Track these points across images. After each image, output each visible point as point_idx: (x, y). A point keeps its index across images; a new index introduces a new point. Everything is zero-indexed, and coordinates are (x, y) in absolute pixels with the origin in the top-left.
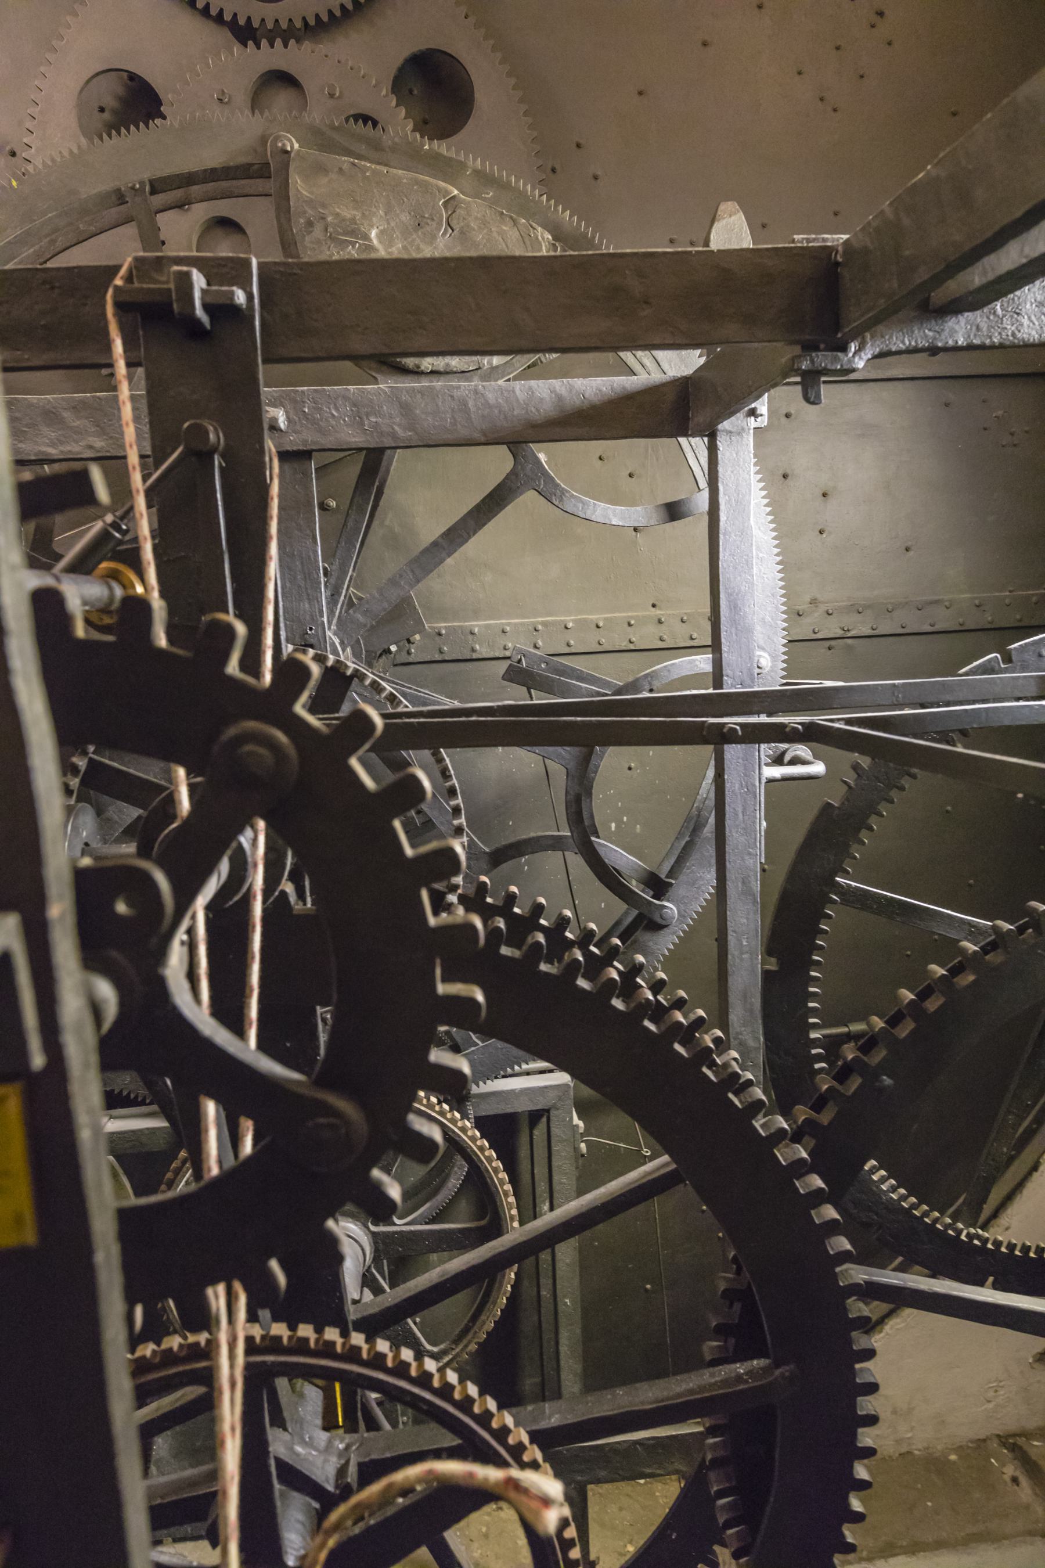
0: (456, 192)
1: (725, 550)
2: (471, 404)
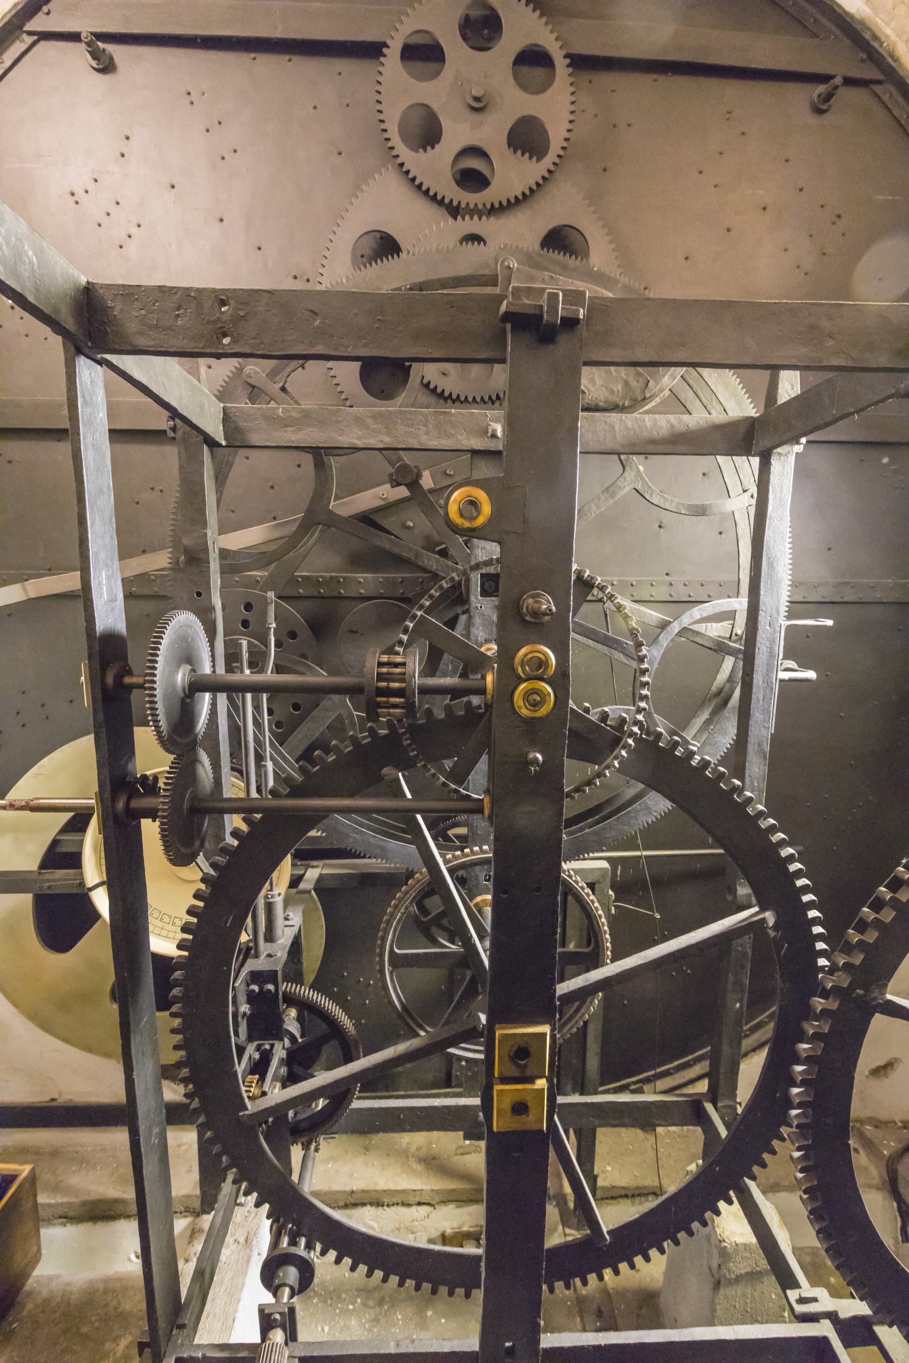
2: (617, 428)
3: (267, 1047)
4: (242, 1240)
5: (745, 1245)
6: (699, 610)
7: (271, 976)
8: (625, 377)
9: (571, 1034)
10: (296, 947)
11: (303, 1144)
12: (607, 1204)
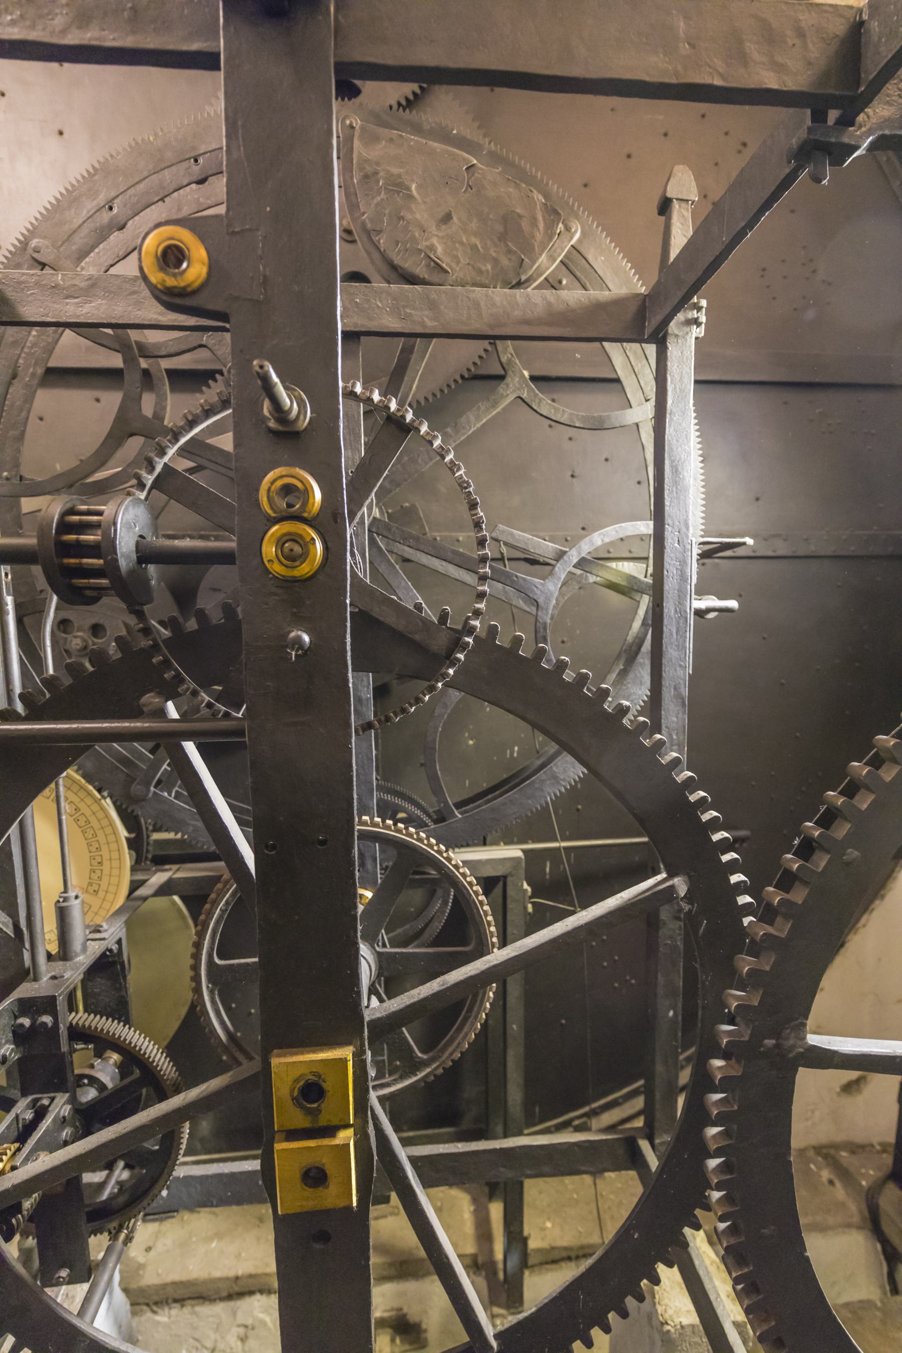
0: (475, 162)
1: (670, 426)
2: (482, 304)
3: (46, 1102)
5: (693, 1326)
6: (600, 535)
7: (48, 1004)
8: (494, 254)
9: (453, 1061)
11: (110, 1233)
12: (547, 1270)
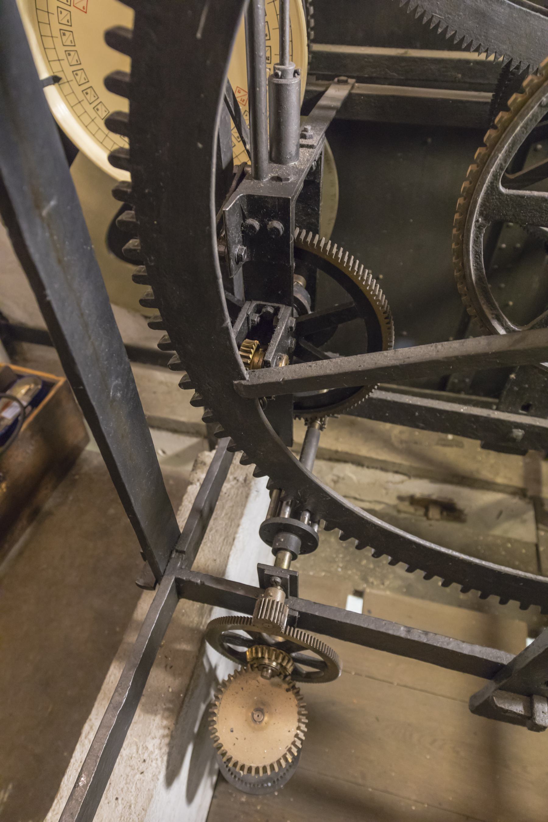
3: (271, 310)
4: (241, 479)
10: (312, 180)
11: (306, 420)
